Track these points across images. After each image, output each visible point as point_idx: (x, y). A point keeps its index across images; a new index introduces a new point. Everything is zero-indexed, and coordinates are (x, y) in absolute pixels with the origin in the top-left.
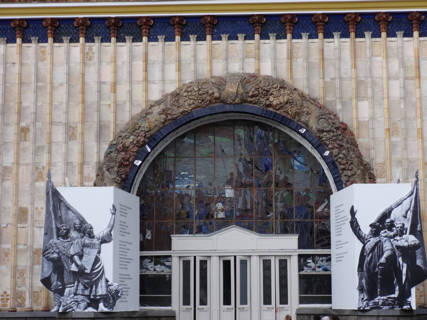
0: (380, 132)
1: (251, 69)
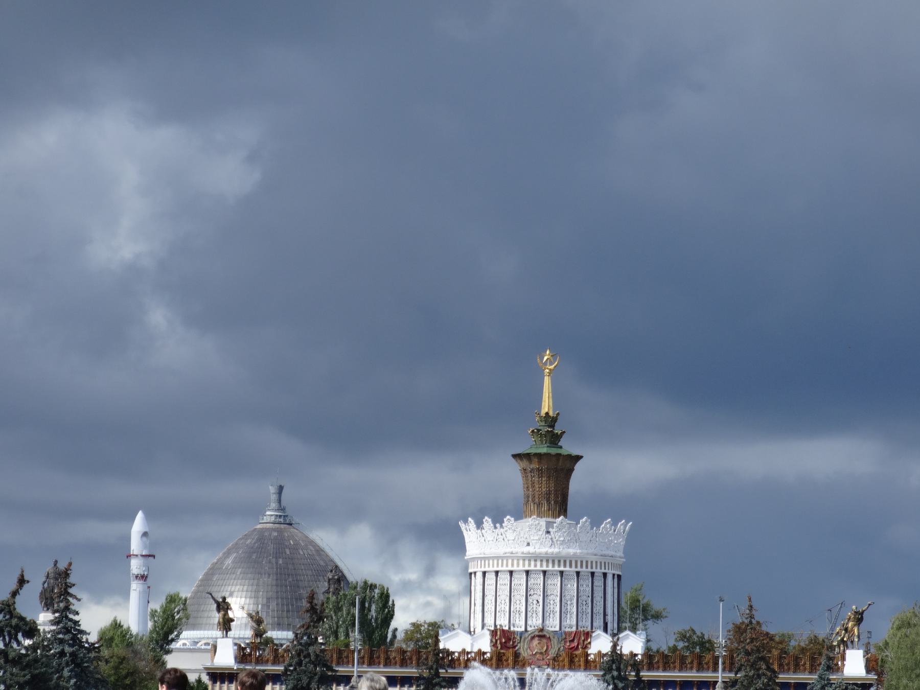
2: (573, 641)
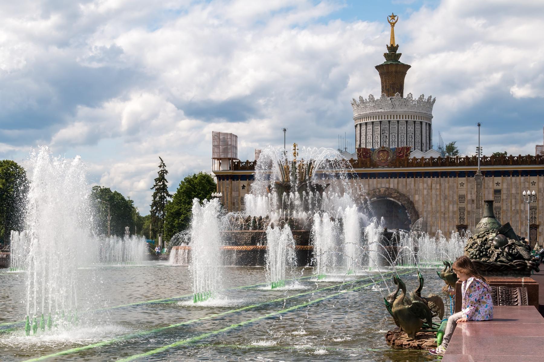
0: (421, 203)
1: (387, 186)
2: (400, 153)
